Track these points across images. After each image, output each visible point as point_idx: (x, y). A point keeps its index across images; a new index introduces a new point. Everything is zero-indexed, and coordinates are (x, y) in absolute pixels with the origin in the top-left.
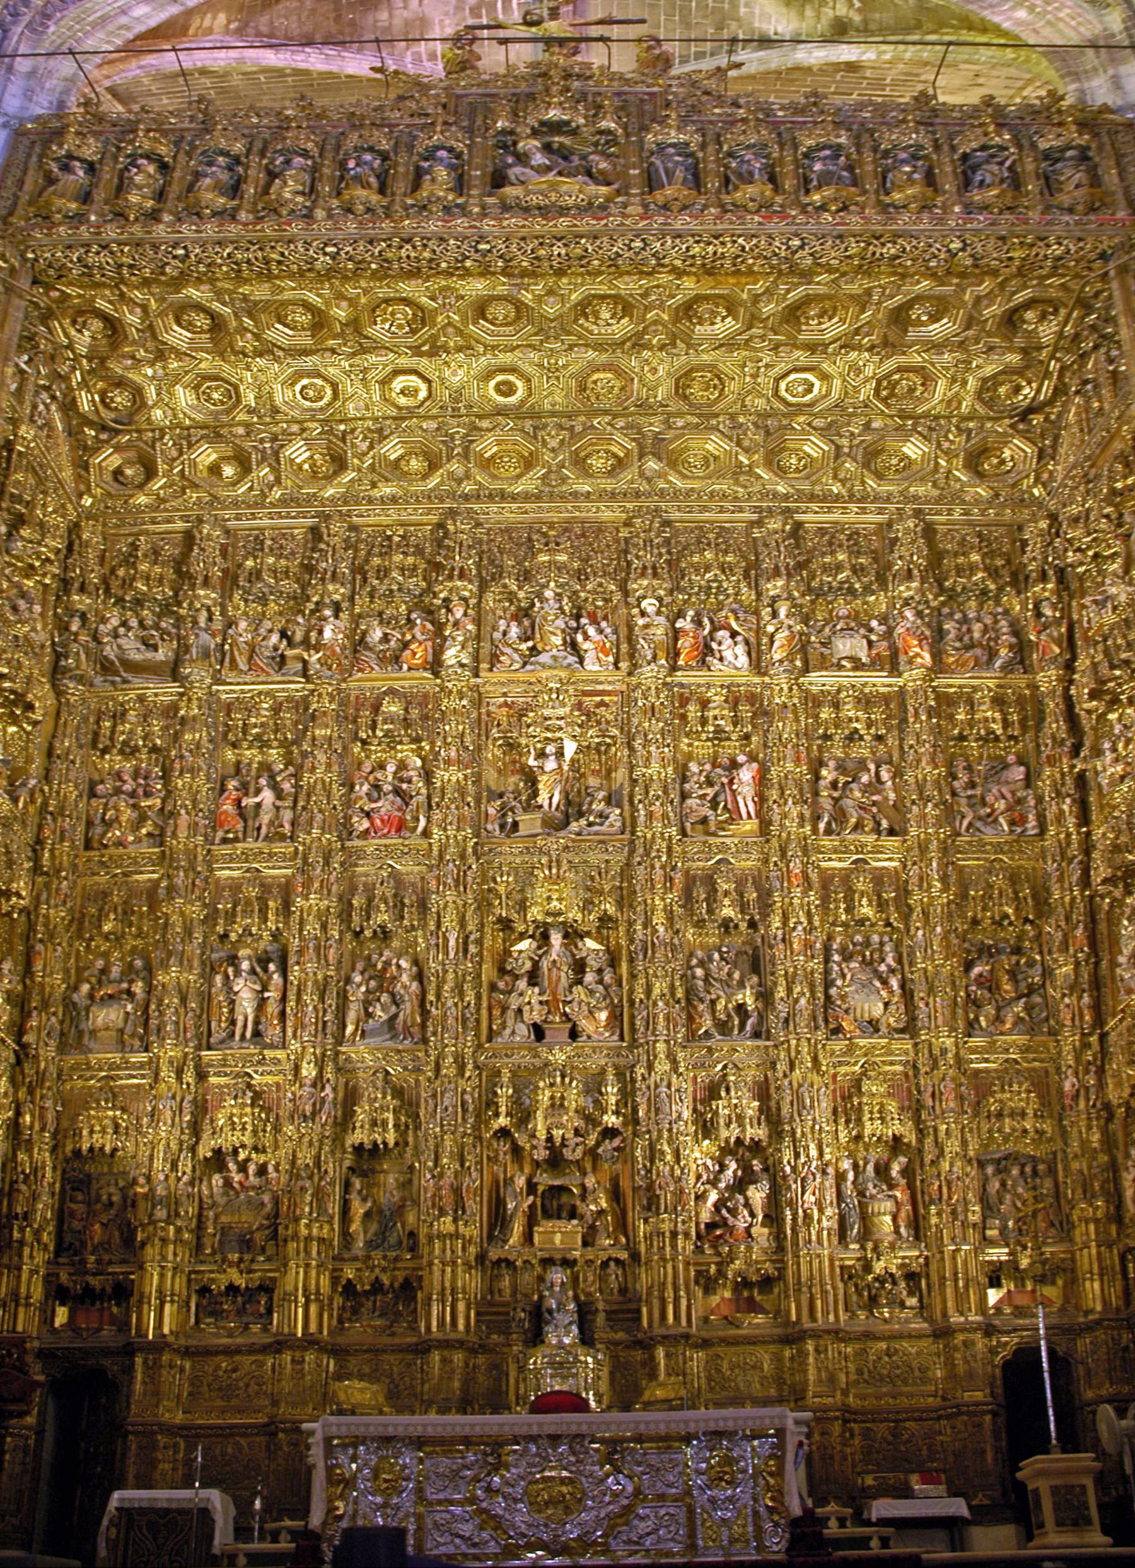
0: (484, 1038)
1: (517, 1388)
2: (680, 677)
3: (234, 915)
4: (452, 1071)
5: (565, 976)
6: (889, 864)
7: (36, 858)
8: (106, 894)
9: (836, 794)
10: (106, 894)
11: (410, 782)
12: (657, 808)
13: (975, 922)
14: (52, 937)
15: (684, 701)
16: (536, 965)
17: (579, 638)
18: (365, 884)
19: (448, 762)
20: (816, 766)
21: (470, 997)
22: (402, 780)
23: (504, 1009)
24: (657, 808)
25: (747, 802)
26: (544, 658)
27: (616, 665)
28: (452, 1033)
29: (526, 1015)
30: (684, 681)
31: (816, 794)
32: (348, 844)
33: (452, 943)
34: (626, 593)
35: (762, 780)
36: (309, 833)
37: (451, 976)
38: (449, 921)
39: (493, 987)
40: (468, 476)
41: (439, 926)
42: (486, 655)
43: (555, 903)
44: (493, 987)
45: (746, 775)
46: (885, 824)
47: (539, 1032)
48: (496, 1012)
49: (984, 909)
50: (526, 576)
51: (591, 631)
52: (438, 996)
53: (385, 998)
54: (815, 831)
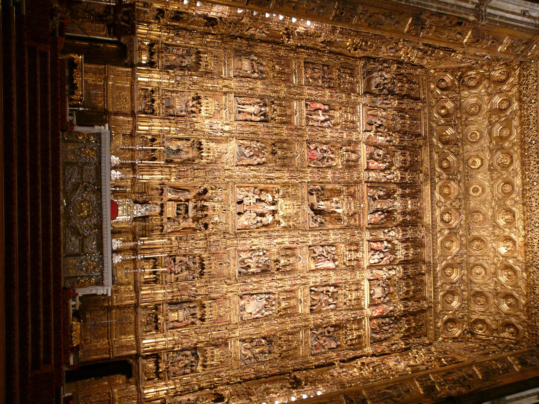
0: (238, 185)
1: (119, 196)
2: (366, 243)
3: (280, 106)
4: (227, 175)
5: (260, 210)
6: (301, 309)
7: (302, 47)
8: (288, 67)
9: (324, 292)
10: (288, 67)
11: (327, 162)
12: (318, 238)
13: (280, 338)
14: (274, 50)
15: (357, 245)
16: (264, 201)
17: (380, 213)
18: (291, 147)
19: (334, 173)
20: (335, 286)
21: (252, 180)
22: (328, 159)
23: (248, 191)
24: (318, 238)
25: (322, 265)
26: (372, 202)
27: (370, 224)
28: (239, 174)
29: (246, 198)
30: (365, 244)
31: (325, 286)
32: (305, 143)
33: (271, 175)
34: (396, 226)
35: (329, 269)
36: (309, 131)
37: (259, 174)
38: (278, 174)
39: (255, 188)
40: (440, 179)
41: (276, 170)
42: (373, 185)
43: (285, 207)
44: (255, 188)
45: (331, 265)
46: (314, 308)
47: (240, 202)
48: (247, 189)
49: (285, 341)
50: (403, 196)
51: (382, 216)
52: (253, 170)
53: (252, 153)
54: (311, 287)
